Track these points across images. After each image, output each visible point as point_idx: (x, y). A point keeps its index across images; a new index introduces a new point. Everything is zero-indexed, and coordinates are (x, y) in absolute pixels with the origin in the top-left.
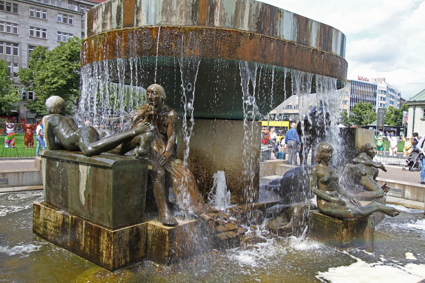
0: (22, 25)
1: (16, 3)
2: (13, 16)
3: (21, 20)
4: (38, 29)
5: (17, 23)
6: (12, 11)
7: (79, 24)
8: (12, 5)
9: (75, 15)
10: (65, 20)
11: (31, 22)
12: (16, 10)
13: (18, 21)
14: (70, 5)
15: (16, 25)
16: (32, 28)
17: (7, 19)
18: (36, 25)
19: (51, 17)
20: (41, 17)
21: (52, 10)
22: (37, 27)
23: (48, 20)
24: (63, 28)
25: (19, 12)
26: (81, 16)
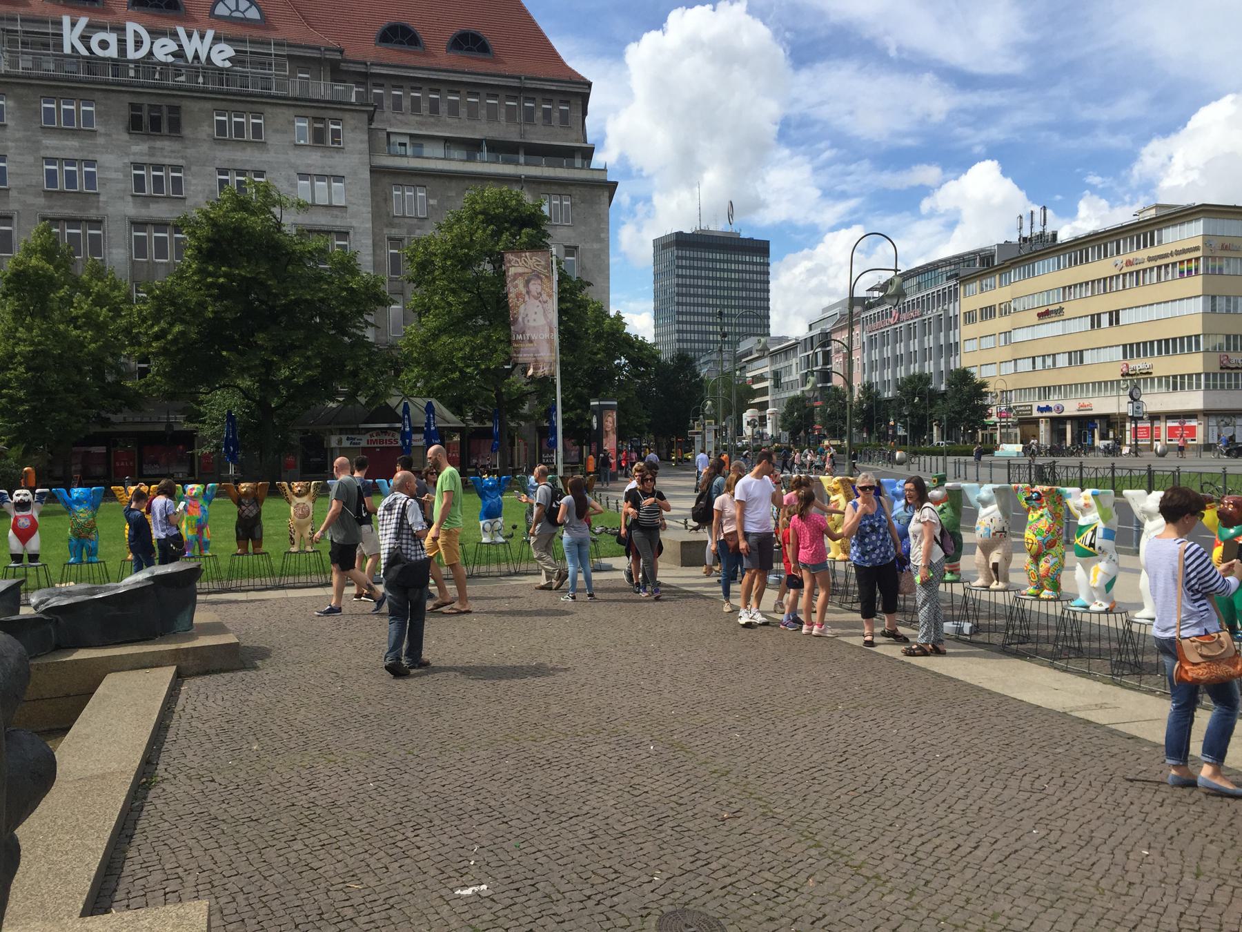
0: (194, 168)
1: (175, 102)
2: (166, 145)
3: (190, 152)
4: (241, 173)
5: (181, 162)
6: (165, 129)
7: (362, 142)
8: (165, 111)
9: (347, 116)
10: (319, 137)
11: (218, 154)
12: (176, 127)
13: (183, 158)
14: (340, 87)
15: (177, 168)
16: (223, 171)
17: (153, 155)
18: (234, 160)
19: (276, 131)
20: (248, 135)
21: (279, 110)
22: (239, 166)
23: (269, 142)
24: (315, 160)
25: (186, 131)
26: (365, 116)
